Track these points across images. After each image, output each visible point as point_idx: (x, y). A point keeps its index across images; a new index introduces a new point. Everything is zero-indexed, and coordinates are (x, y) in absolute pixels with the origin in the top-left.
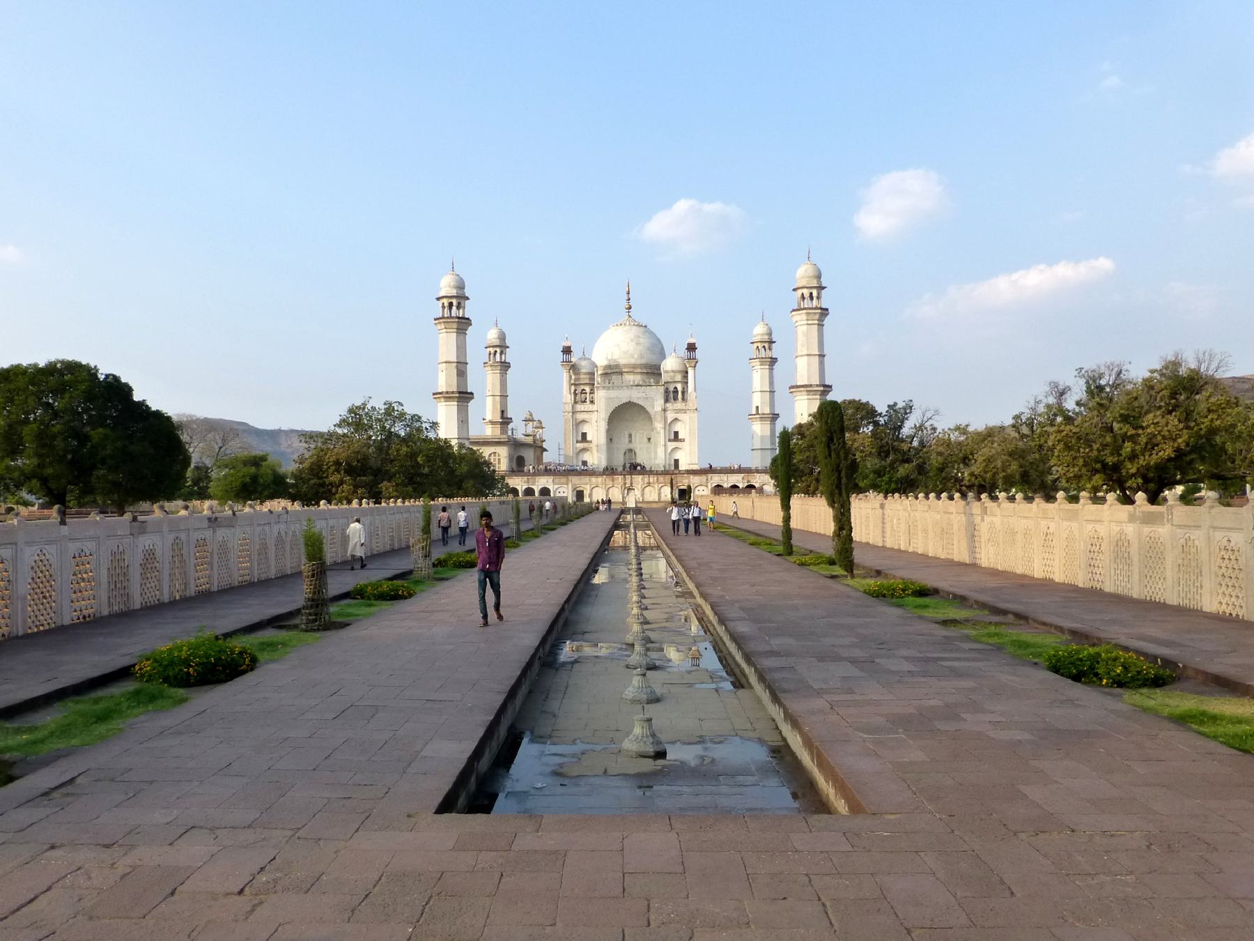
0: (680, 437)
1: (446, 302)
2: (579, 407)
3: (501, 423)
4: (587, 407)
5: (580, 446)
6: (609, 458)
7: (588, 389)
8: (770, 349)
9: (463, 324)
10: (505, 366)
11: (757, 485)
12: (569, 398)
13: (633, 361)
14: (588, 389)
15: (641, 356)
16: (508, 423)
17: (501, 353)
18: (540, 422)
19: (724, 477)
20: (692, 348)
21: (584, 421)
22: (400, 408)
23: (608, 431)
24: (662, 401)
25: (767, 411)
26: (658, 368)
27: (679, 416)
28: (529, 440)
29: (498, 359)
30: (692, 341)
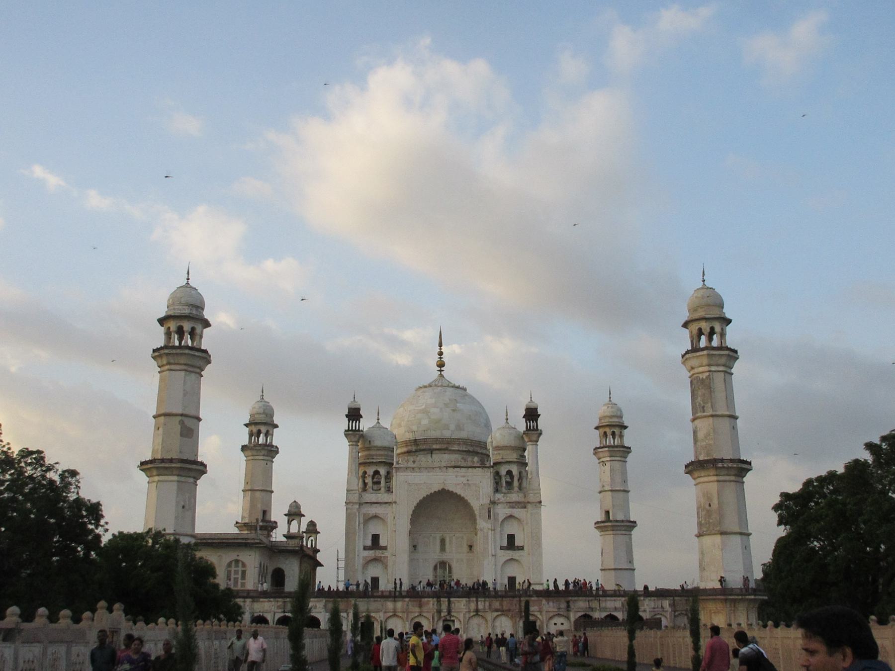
0: (518, 543)
1: (173, 326)
2: (370, 497)
3: (262, 528)
4: (383, 496)
5: (371, 554)
6: (411, 576)
7: (383, 471)
8: (621, 436)
9: (197, 359)
10: (271, 451)
13: (447, 434)
14: (383, 471)
15: (459, 428)
17: (267, 435)
18: (312, 524)
19: (595, 604)
20: (532, 414)
21: (376, 517)
23: (410, 533)
25: (620, 517)
26: (483, 445)
28: (293, 543)
30: (532, 406)
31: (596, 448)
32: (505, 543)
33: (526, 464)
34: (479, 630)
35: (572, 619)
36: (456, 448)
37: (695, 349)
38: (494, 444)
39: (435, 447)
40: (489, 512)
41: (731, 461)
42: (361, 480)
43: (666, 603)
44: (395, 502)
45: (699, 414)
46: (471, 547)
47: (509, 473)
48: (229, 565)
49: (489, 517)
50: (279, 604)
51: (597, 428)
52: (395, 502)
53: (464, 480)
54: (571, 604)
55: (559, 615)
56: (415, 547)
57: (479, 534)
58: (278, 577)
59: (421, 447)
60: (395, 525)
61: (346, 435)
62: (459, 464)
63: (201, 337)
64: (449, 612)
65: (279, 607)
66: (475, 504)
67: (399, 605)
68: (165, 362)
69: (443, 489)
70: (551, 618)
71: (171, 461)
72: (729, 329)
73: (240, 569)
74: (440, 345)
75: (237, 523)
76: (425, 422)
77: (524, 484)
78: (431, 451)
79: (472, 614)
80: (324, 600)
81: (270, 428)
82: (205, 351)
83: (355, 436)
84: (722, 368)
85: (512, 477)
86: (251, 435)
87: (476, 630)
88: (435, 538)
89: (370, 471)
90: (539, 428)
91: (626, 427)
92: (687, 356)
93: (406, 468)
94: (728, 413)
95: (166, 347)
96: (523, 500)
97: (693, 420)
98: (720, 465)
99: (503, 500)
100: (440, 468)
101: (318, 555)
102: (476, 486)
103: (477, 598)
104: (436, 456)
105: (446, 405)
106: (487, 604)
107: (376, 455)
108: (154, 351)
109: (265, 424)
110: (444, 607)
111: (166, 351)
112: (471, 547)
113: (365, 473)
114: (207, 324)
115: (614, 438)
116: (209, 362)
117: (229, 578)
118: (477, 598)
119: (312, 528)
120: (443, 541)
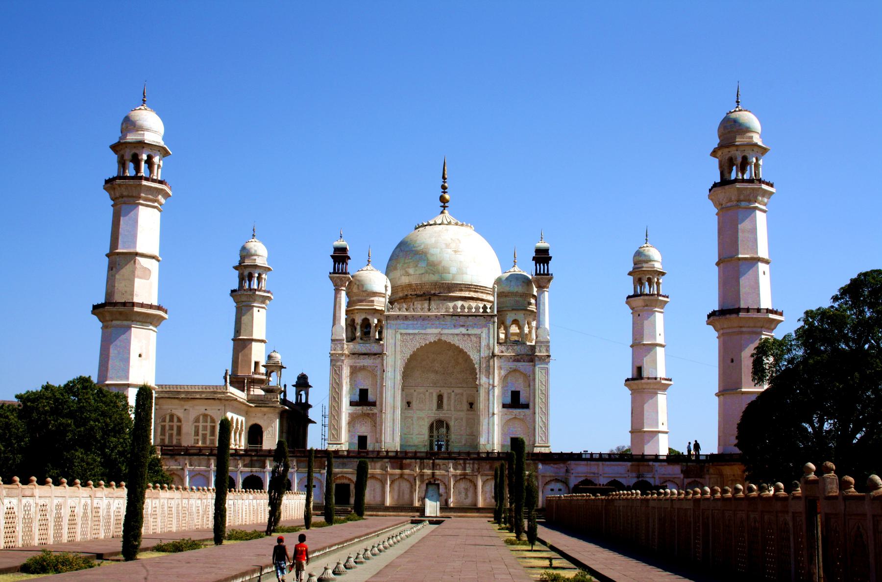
0: (523, 400)
13: (449, 279)
20: (542, 257)
30: (542, 245)
31: (629, 297)
32: (508, 400)
34: (466, 494)
37: (725, 182)
42: (349, 329)
46: (471, 405)
48: (197, 420)
51: (630, 274)
55: (557, 480)
56: (409, 404)
61: (331, 278)
64: (433, 474)
65: (245, 466)
66: (474, 356)
68: (118, 195)
69: (440, 340)
70: (547, 484)
73: (209, 424)
79: (459, 478)
86: (242, 279)
87: (463, 494)
89: (359, 320)
90: (550, 272)
95: (119, 177)
97: (718, 264)
101: (310, 411)
103: (465, 459)
106: (476, 466)
108: (107, 182)
109: (256, 266)
110: (428, 472)
112: (471, 405)
113: (353, 321)
117: (197, 433)
118: (465, 459)
119: (302, 383)
120: (440, 398)
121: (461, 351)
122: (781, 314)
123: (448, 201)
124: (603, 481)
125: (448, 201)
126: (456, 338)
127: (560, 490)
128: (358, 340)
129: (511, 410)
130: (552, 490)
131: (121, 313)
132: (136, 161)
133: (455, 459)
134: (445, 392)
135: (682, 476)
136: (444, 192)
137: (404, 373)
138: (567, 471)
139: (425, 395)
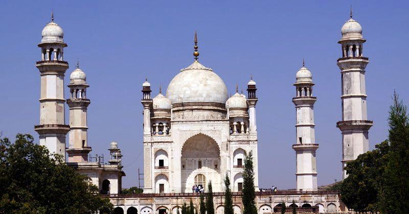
2: (158, 138)
4: (164, 138)
5: (160, 171)
8: (310, 91)
11: (313, 205)
12: (147, 129)
13: (201, 100)
15: (208, 96)
16: (88, 152)
22: (30, 140)
23: (182, 157)
24: (228, 133)
26: (223, 105)
27: (243, 147)
28: (114, 167)
29: (80, 97)
30: (252, 83)
33: (249, 118)
35: (273, 207)
36: (207, 107)
38: (230, 107)
39: (194, 107)
40: (227, 146)
41: (361, 121)
43: (323, 198)
44: (173, 142)
45: (345, 95)
46: (216, 166)
47: (239, 123)
49: (227, 149)
50: (115, 201)
52: (173, 142)
53: (213, 129)
54: (272, 198)
57: (222, 159)
58: (105, 185)
59: (186, 107)
60: (172, 154)
62: (209, 119)
63: (63, 53)
67: (179, 200)
69: (200, 134)
70: (261, 207)
71: (53, 125)
72: (364, 44)
74: (196, 43)
75: (66, 148)
76: (188, 92)
77: (247, 130)
78: (192, 110)
79: (219, 205)
80: (139, 198)
81: (83, 88)
82: (66, 63)
83: (147, 103)
84: (359, 69)
85: (241, 125)
88: (195, 161)
90: (256, 97)
91: (313, 85)
92: (340, 61)
93: (178, 122)
94: (361, 95)
96: (247, 139)
98: (355, 124)
99: (235, 139)
100: (198, 121)
102: (220, 132)
104: (195, 113)
105: (201, 82)
107: (160, 114)
111: (45, 64)
112: (216, 166)
114: (66, 46)
115: (306, 91)
116: (68, 67)
118: (221, 196)
121: (210, 139)
122: (372, 122)
123: (198, 55)
124: (287, 205)
125: (198, 55)
126: (209, 132)
127: (267, 209)
128: (157, 134)
129: (238, 169)
130: (264, 209)
131: (51, 130)
132: (52, 50)
133: (217, 196)
134: (202, 159)
135: (325, 201)
136: (196, 51)
137: (182, 151)
138: (271, 200)
139: (192, 161)
